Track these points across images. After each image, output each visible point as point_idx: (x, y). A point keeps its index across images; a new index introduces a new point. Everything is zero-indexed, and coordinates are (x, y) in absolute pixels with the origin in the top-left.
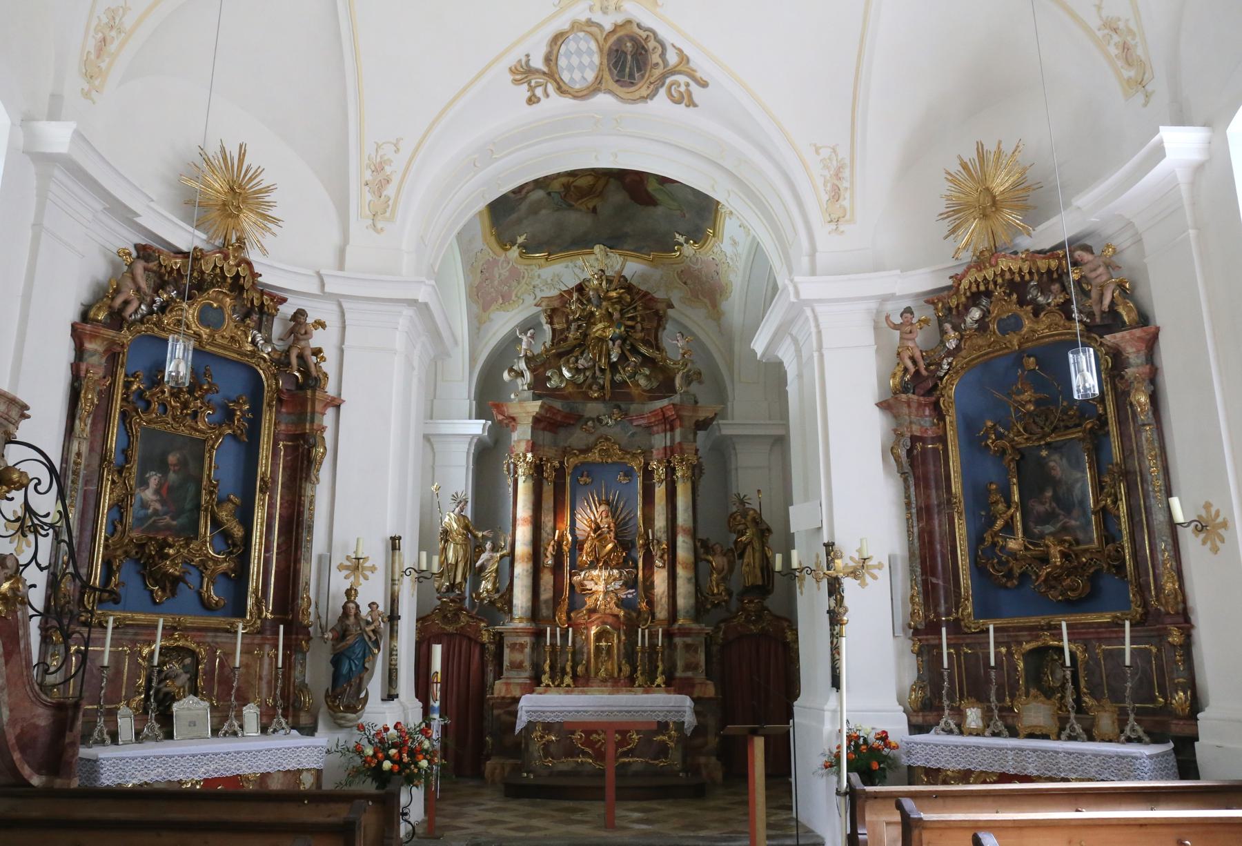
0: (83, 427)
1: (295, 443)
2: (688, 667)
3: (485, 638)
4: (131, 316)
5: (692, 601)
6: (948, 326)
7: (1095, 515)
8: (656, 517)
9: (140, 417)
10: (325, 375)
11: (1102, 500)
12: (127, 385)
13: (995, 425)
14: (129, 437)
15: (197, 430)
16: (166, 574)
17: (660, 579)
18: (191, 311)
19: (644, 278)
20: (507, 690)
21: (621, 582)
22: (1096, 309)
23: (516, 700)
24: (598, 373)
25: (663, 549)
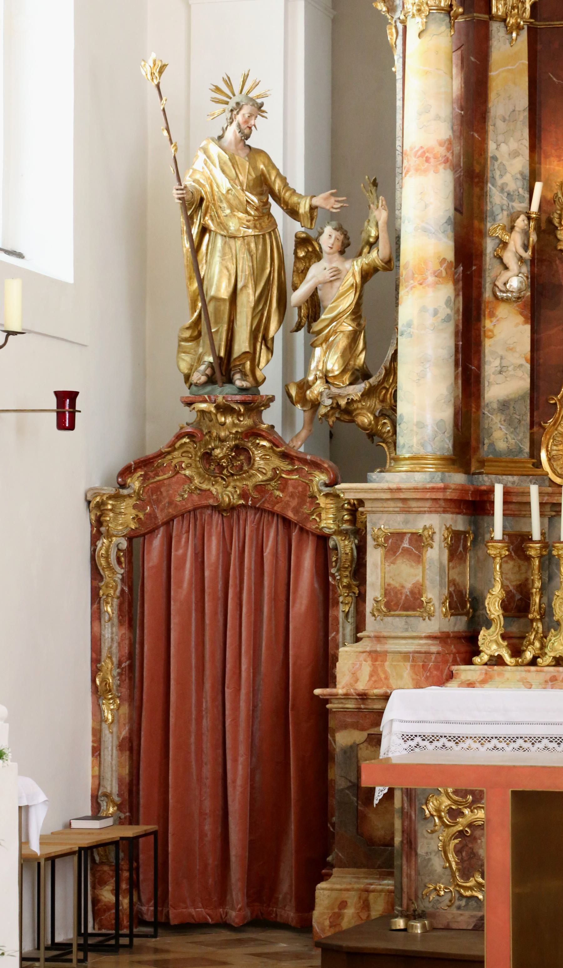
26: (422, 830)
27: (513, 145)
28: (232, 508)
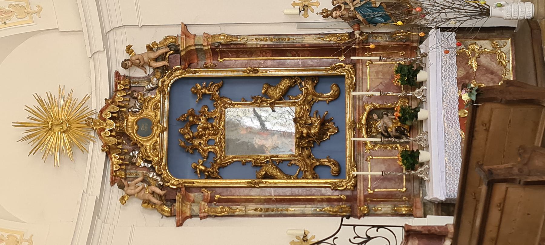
10: (165, 39)
18: (145, 144)
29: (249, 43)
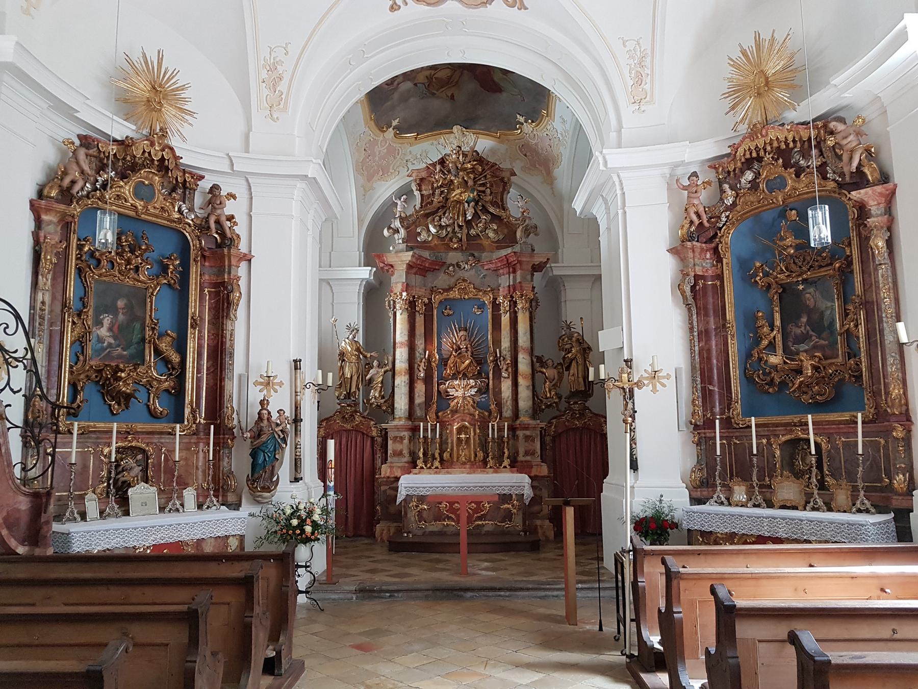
0: (45, 281)
1: (218, 290)
2: (527, 453)
3: (374, 434)
4: (78, 193)
5: (530, 403)
6: (726, 186)
7: (841, 336)
8: (502, 340)
9: (93, 272)
11: (846, 324)
12: (80, 247)
13: (762, 265)
14: (85, 287)
15: (139, 281)
16: (119, 392)
17: (506, 387)
19: (493, 151)
20: (391, 471)
21: (476, 390)
22: (846, 170)
23: (397, 479)
24: (457, 229)
25: (508, 364)
26: (409, 511)
27: (421, 342)
28: (349, 430)
29: (229, 322)
